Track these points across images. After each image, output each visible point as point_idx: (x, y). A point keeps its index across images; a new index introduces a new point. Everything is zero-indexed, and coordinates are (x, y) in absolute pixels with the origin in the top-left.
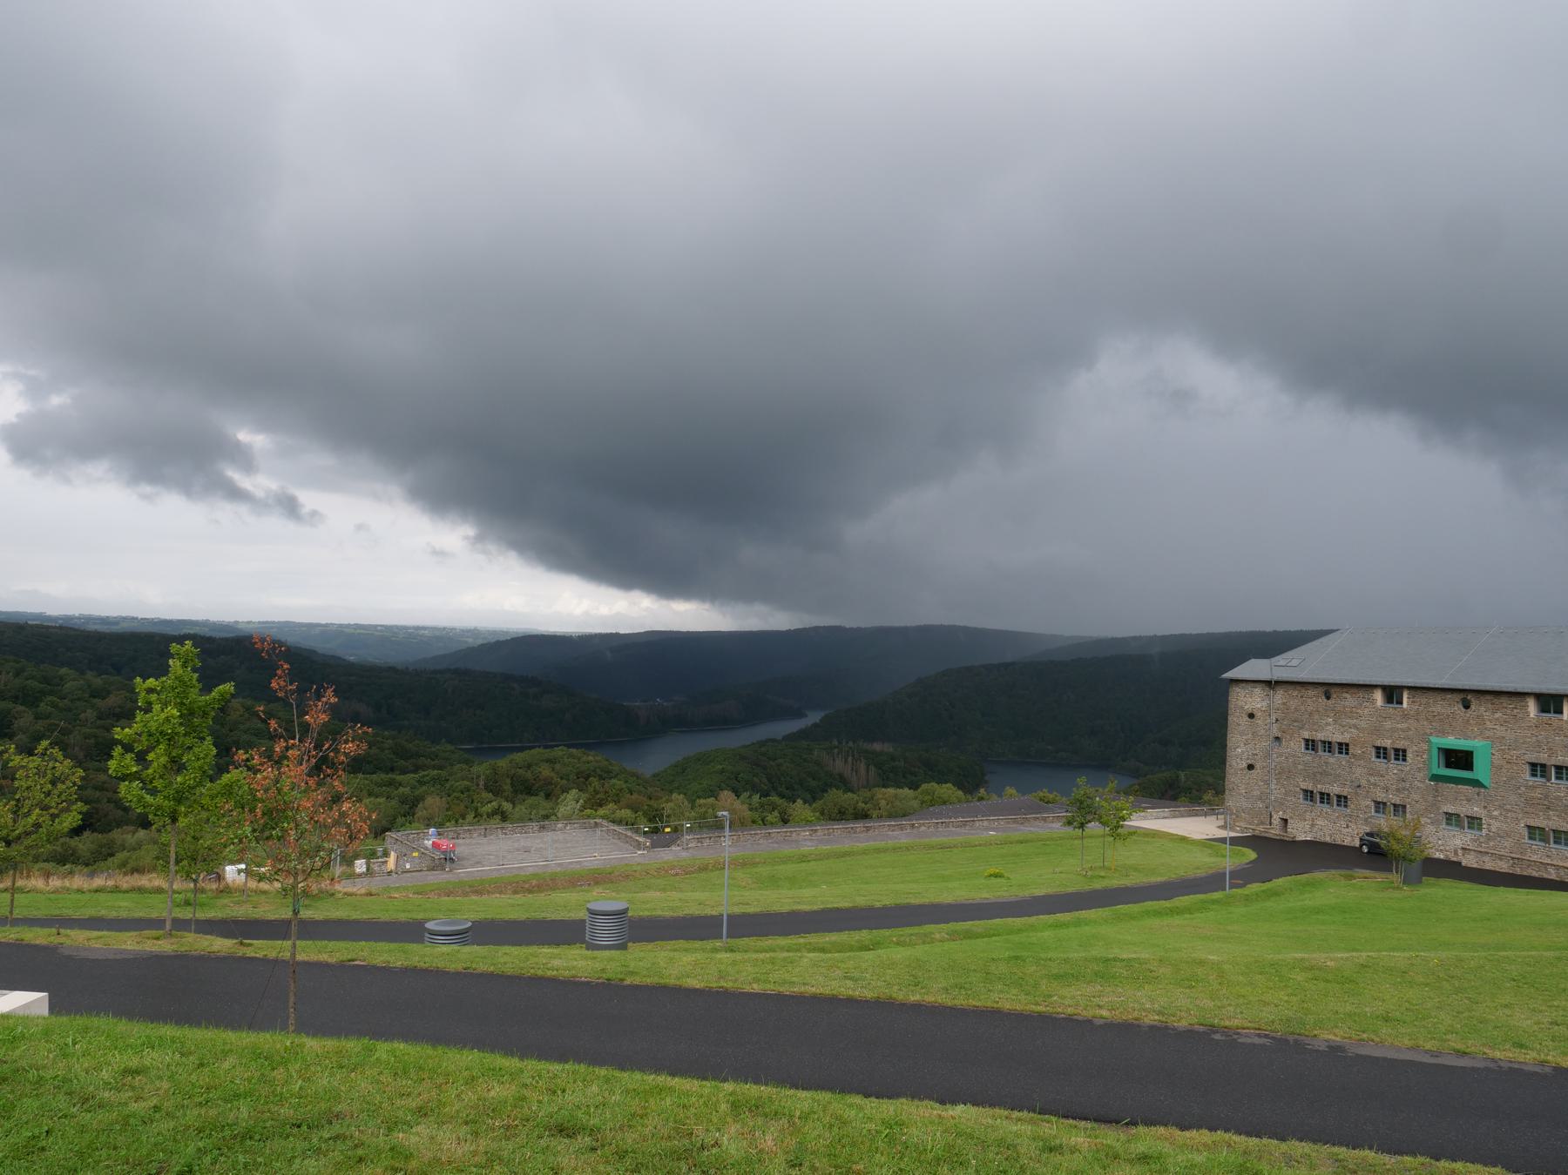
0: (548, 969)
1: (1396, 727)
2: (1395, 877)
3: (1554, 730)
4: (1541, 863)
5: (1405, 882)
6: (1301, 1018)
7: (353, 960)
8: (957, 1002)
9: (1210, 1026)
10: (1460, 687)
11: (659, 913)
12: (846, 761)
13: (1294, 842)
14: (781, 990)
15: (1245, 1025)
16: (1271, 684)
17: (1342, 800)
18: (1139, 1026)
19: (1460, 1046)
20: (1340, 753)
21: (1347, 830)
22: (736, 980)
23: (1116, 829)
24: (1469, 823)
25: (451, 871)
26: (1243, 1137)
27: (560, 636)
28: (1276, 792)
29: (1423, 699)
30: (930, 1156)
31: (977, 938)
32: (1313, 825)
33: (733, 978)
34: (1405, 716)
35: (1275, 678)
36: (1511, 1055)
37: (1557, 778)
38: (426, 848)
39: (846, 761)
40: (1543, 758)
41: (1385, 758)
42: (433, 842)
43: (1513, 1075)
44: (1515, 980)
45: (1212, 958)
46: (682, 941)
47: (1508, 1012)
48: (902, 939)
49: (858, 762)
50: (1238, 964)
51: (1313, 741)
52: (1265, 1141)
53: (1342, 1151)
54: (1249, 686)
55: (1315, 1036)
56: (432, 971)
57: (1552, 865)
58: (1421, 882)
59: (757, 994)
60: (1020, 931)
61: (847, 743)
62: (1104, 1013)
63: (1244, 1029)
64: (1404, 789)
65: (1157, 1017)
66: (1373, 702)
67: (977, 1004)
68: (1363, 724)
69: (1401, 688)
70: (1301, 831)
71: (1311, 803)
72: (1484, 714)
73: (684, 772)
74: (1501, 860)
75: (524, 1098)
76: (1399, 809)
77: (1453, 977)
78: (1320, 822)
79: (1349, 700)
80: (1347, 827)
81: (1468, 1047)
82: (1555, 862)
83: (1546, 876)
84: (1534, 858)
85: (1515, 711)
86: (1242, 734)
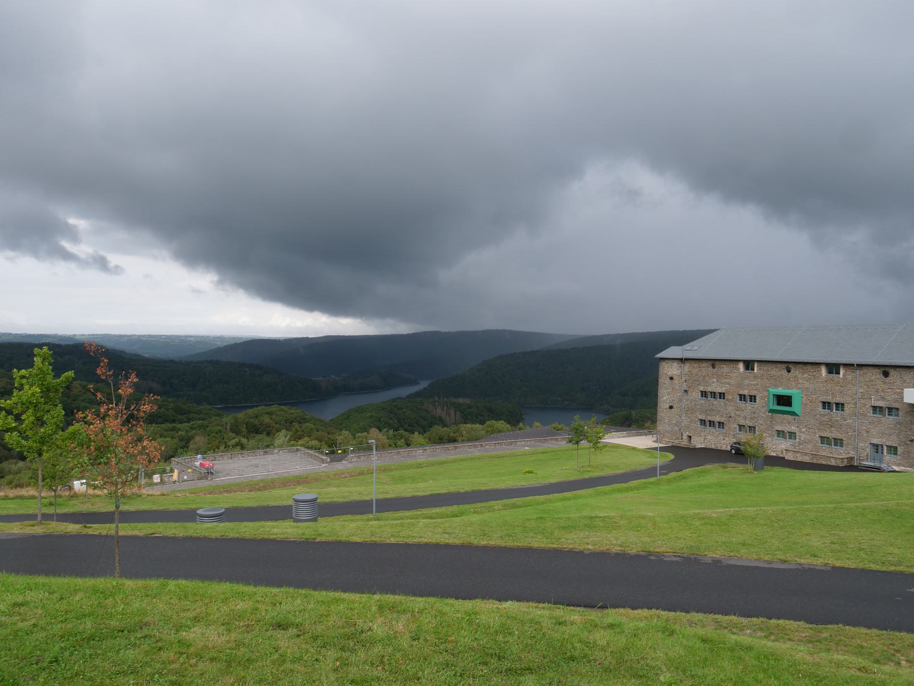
0: (271, 535)
1: (752, 383)
2: (749, 467)
3: (835, 383)
4: (827, 456)
5: (755, 469)
6: (698, 546)
7: (153, 534)
8: (508, 544)
9: (649, 552)
11: (335, 500)
12: (443, 409)
13: (695, 449)
15: (668, 551)
16: (681, 360)
17: (721, 425)
18: (609, 554)
19: (783, 558)
20: (720, 398)
22: (381, 537)
23: (596, 444)
24: (789, 436)
25: (211, 479)
26: (666, 612)
27: (273, 340)
28: (685, 421)
30: (492, 630)
32: (705, 439)
33: (379, 535)
34: (756, 377)
35: (685, 357)
36: (810, 561)
37: (836, 410)
38: (196, 467)
39: (443, 409)
40: (829, 399)
41: (744, 401)
42: (200, 463)
44: (812, 521)
46: (349, 515)
47: (808, 538)
48: (476, 510)
49: (450, 410)
51: (705, 392)
52: (678, 613)
53: (719, 617)
54: (670, 362)
55: (706, 555)
56: (201, 538)
57: (833, 457)
58: (762, 469)
59: (393, 544)
60: (543, 503)
61: (443, 399)
62: (590, 547)
64: (754, 418)
65: (619, 548)
66: (739, 369)
67: (520, 545)
68: (733, 382)
69: (754, 361)
70: (698, 443)
72: (798, 375)
73: (348, 418)
74: (806, 455)
75: (257, 609)
76: (752, 429)
77: (779, 520)
78: (709, 437)
79: (725, 369)
80: (724, 440)
81: (787, 558)
82: (834, 456)
83: (829, 463)
84: (824, 454)
85: (815, 373)
86: (666, 389)
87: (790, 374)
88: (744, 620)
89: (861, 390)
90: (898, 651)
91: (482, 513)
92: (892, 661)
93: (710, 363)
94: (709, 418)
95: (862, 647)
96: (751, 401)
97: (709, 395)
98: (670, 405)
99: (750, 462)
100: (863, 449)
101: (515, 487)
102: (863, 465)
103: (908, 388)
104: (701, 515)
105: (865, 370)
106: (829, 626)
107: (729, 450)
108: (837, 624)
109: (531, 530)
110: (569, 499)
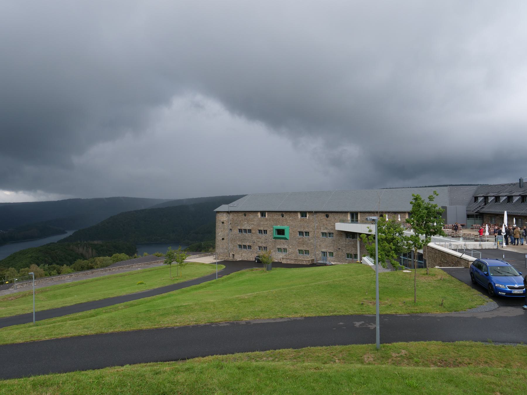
2: (264, 269)
5: (268, 270)
10: (281, 211)
13: (236, 261)
14: (58, 337)
16: (228, 212)
17: (250, 247)
18: (189, 327)
19: (281, 316)
20: (249, 232)
21: (251, 256)
22: (38, 337)
24: (284, 250)
26: (222, 356)
29: (271, 215)
31: (135, 306)
33: (37, 336)
34: (266, 220)
35: (230, 210)
36: (294, 316)
37: (306, 235)
40: (302, 230)
41: (261, 233)
43: (294, 322)
45: (211, 301)
47: (293, 304)
48: (107, 310)
50: (219, 302)
51: (241, 229)
52: (228, 355)
53: (250, 353)
54: (222, 213)
55: (242, 320)
60: (150, 301)
62: (178, 324)
63: (221, 322)
64: (267, 242)
65: (195, 323)
67: (134, 329)
68: (255, 223)
69: (265, 212)
70: (238, 258)
71: (241, 249)
74: (292, 260)
76: (265, 248)
77: (279, 296)
78: (244, 254)
79: (251, 216)
82: (305, 260)
83: (303, 264)
87: (283, 218)
88: (262, 353)
89: (317, 225)
90: (334, 355)
91: (111, 312)
92: (332, 361)
93: (243, 213)
94: (244, 244)
95: (319, 356)
96: (264, 233)
97: (243, 231)
98: (223, 237)
99: (265, 266)
100: (318, 255)
101: (132, 294)
102: (318, 263)
103: (337, 222)
104: (240, 298)
105: (318, 214)
106: (304, 348)
107: (254, 260)
108: (307, 347)
109: (142, 319)
110: (166, 297)
